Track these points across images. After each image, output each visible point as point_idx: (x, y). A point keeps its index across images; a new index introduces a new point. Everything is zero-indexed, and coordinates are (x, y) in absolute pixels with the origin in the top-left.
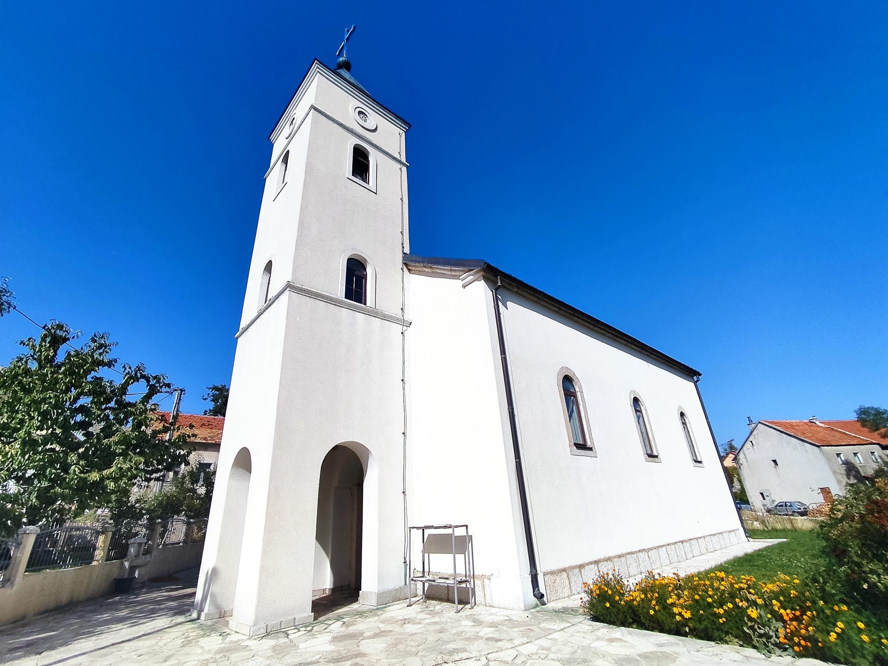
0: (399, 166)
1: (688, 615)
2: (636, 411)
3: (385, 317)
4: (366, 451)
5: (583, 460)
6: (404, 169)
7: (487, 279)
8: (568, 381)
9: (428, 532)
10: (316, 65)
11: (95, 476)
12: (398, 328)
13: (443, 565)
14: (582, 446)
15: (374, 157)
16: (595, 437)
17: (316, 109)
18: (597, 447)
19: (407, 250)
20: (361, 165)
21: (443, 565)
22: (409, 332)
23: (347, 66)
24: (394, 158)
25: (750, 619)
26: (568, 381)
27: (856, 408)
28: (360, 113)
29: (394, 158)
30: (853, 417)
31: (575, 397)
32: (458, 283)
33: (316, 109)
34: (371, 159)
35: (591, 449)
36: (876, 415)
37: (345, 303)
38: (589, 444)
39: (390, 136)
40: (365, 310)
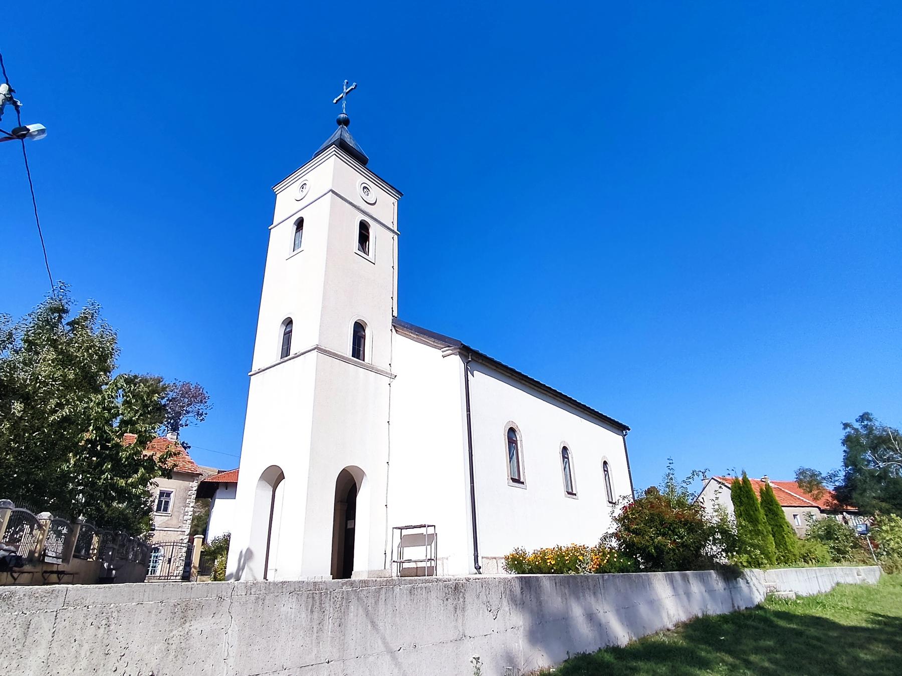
0: (392, 234)
1: (553, 563)
2: (564, 457)
3: (378, 372)
4: (362, 473)
5: (517, 490)
6: (396, 237)
7: (460, 354)
8: (512, 431)
9: (405, 532)
10: (333, 149)
11: (122, 482)
12: (387, 380)
13: (416, 554)
14: (517, 481)
15: (374, 231)
16: (527, 475)
17: (333, 192)
18: (527, 482)
19: (395, 314)
20: (364, 238)
21: (416, 554)
22: (394, 383)
23: (346, 122)
24: (389, 228)
25: (580, 561)
26: (512, 431)
27: (796, 468)
28: (365, 188)
29: (389, 228)
30: (792, 478)
31: (516, 444)
32: (439, 353)
33: (333, 192)
34: (371, 231)
35: (523, 483)
36: (811, 477)
37: (349, 360)
38: (522, 480)
39: (385, 206)
40: (362, 365)
